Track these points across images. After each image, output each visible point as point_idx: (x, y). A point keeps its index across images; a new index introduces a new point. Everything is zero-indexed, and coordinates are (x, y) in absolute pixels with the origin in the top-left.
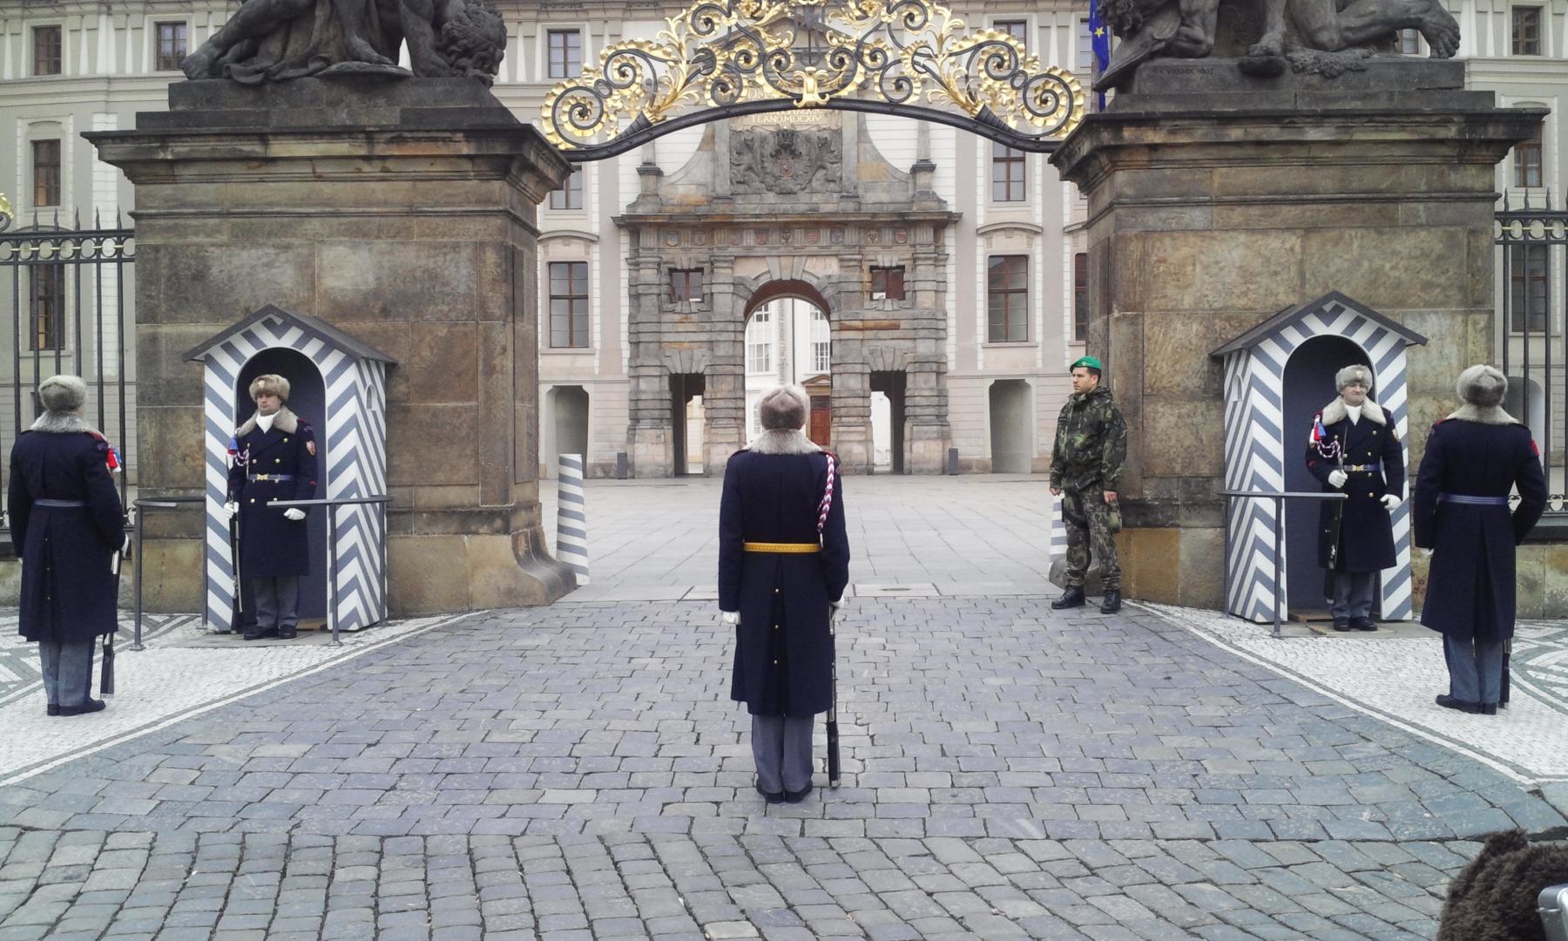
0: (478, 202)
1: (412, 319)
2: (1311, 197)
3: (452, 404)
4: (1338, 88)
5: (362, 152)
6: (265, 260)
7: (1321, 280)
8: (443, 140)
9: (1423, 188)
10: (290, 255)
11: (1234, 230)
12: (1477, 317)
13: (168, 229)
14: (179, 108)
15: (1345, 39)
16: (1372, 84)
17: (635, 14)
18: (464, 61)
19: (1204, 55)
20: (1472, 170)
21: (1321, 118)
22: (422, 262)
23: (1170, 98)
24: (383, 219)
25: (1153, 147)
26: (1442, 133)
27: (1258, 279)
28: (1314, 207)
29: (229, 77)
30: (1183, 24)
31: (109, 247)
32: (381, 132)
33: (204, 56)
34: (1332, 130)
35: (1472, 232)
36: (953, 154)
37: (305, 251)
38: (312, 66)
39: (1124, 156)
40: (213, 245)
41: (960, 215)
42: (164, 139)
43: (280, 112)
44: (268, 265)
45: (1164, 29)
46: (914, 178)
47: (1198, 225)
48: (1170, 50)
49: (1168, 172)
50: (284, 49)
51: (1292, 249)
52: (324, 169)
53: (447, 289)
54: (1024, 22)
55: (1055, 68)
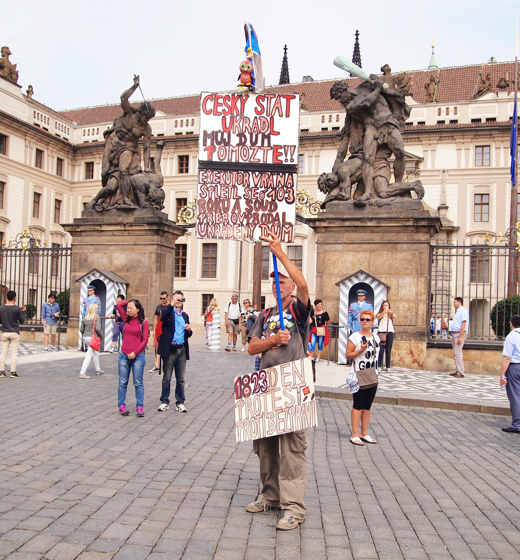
0: (151, 241)
1: (134, 272)
2: (372, 242)
3: (142, 295)
4: (383, 210)
5: (123, 229)
6: (101, 256)
7: (374, 266)
8: (142, 225)
9: (406, 240)
10: (107, 255)
11: (350, 251)
12: (421, 278)
13: (79, 248)
14: (84, 217)
15: (388, 195)
16: (393, 208)
17: (325, 148)
18: (153, 203)
19: (347, 200)
20: (421, 234)
21: (371, 219)
22: (137, 257)
23: (333, 213)
24: (128, 246)
25: (326, 227)
26: (407, 224)
27: (356, 265)
28: (374, 245)
29: (95, 209)
30: (340, 191)
31: (64, 252)
32: (127, 224)
33: (91, 203)
34: (375, 223)
35: (420, 253)
36: (456, 201)
37: (110, 254)
38: (116, 206)
39: (318, 230)
40: (89, 252)
41: (459, 228)
42: (78, 226)
43: (106, 218)
44: (102, 258)
45: (335, 192)
46: (439, 211)
47: (340, 249)
48: (336, 198)
49: (332, 234)
50: (110, 201)
51: (366, 257)
52: (115, 233)
53: (142, 265)
54: (489, 146)
55: (318, 201)
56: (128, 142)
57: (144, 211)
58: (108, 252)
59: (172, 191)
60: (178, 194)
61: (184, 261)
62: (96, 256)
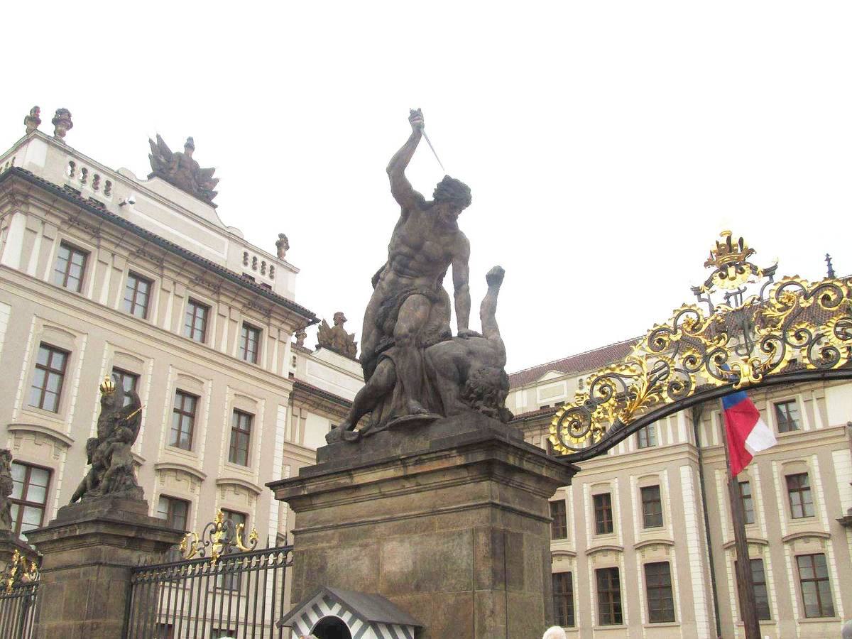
5: (401, 473)
6: (355, 555)
10: (368, 550)
14: (320, 463)
18: (479, 403)
22: (440, 548)
37: (375, 547)
40: (330, 548)
43: (368, 455)
44: (356, 559)
53: (455, 567)
56: (417, 277)
57: (454, 423)
58: (370, 541)
59: (585, 485)
60: (595, 488)
61: (617, 595)
62: (346, 553)
